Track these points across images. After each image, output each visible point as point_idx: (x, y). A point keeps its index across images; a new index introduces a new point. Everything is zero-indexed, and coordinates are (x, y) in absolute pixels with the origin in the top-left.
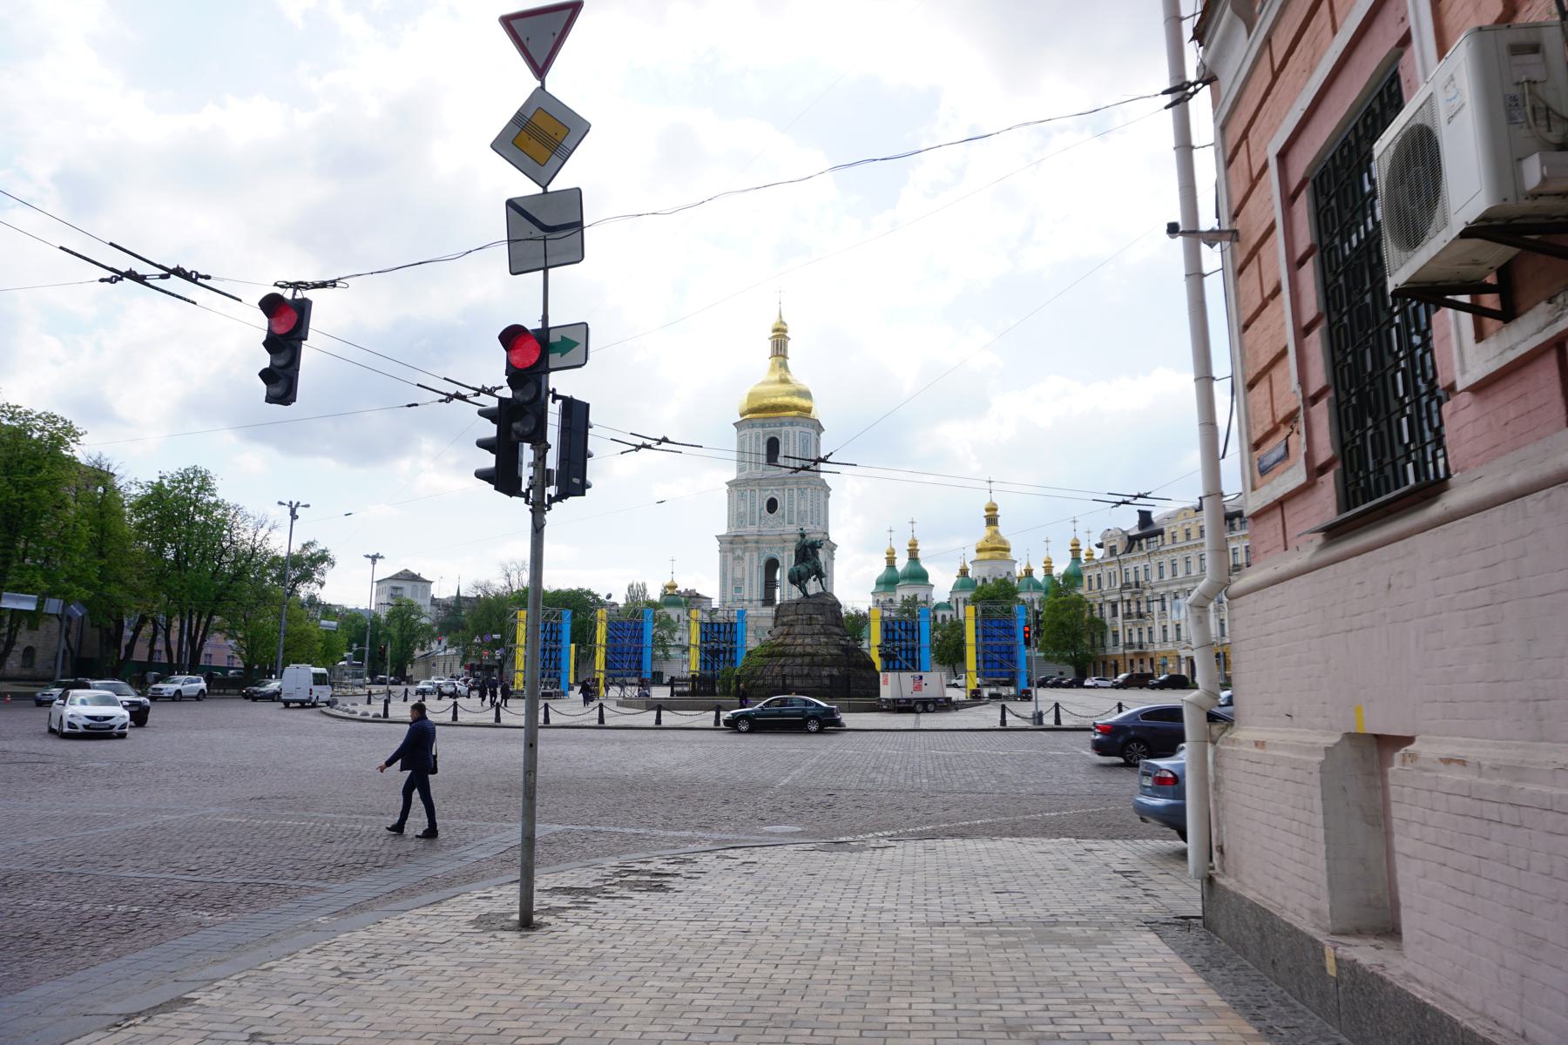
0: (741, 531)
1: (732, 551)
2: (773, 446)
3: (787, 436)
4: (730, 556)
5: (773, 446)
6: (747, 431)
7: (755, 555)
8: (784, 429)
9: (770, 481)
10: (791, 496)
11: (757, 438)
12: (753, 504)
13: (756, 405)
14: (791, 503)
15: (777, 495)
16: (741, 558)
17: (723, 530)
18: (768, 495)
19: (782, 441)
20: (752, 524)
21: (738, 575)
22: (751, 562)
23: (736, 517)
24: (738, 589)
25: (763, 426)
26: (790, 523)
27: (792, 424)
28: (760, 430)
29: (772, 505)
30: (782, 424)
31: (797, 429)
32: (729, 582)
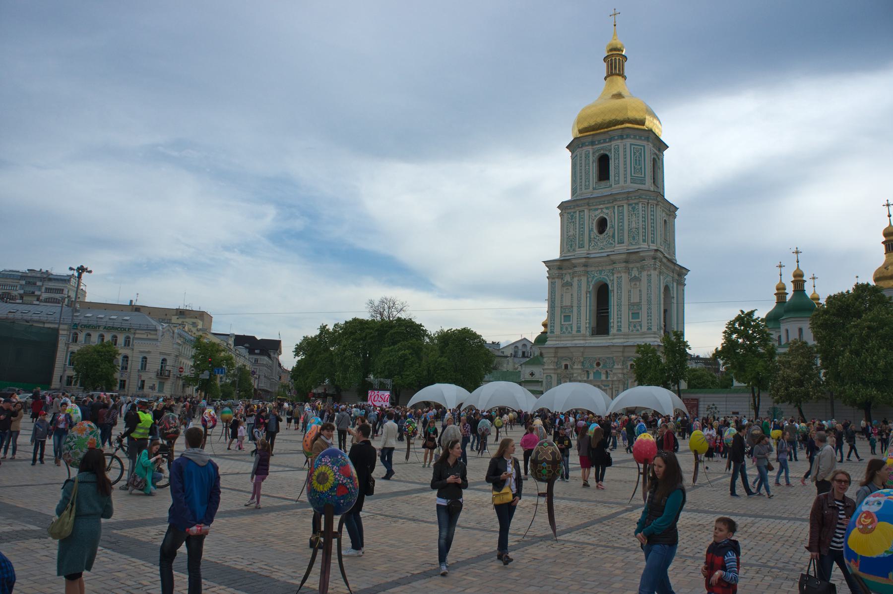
0: (569, 255)
1: (561, 277)
2: (604, 162)
3: (617, 150)
4: (558, 282)
5: (604, 162)
6: (578, 151)
7: (584, 279)
8: (614, 143)
9: (601, 200)
10: (621, 213)
11: (587, 156)
12: (582, 225)
13: (586, 125)
14: (621, 220)
15: (605, 213)
16: (569, 284)
17: (555, 254)
18: (598, 214)
19: (612, 156)
20: (582, 246)
21: (567, 302)
22: (579, 287)
23: (568, 240)
24: (567, 318)
25: (592, 143)
26: (621, 242)
27: (621, 137)
28: (590, 149)
29: (602, 225)
30: (611, 139)
31: (628, 142)
32: (558, 310)
